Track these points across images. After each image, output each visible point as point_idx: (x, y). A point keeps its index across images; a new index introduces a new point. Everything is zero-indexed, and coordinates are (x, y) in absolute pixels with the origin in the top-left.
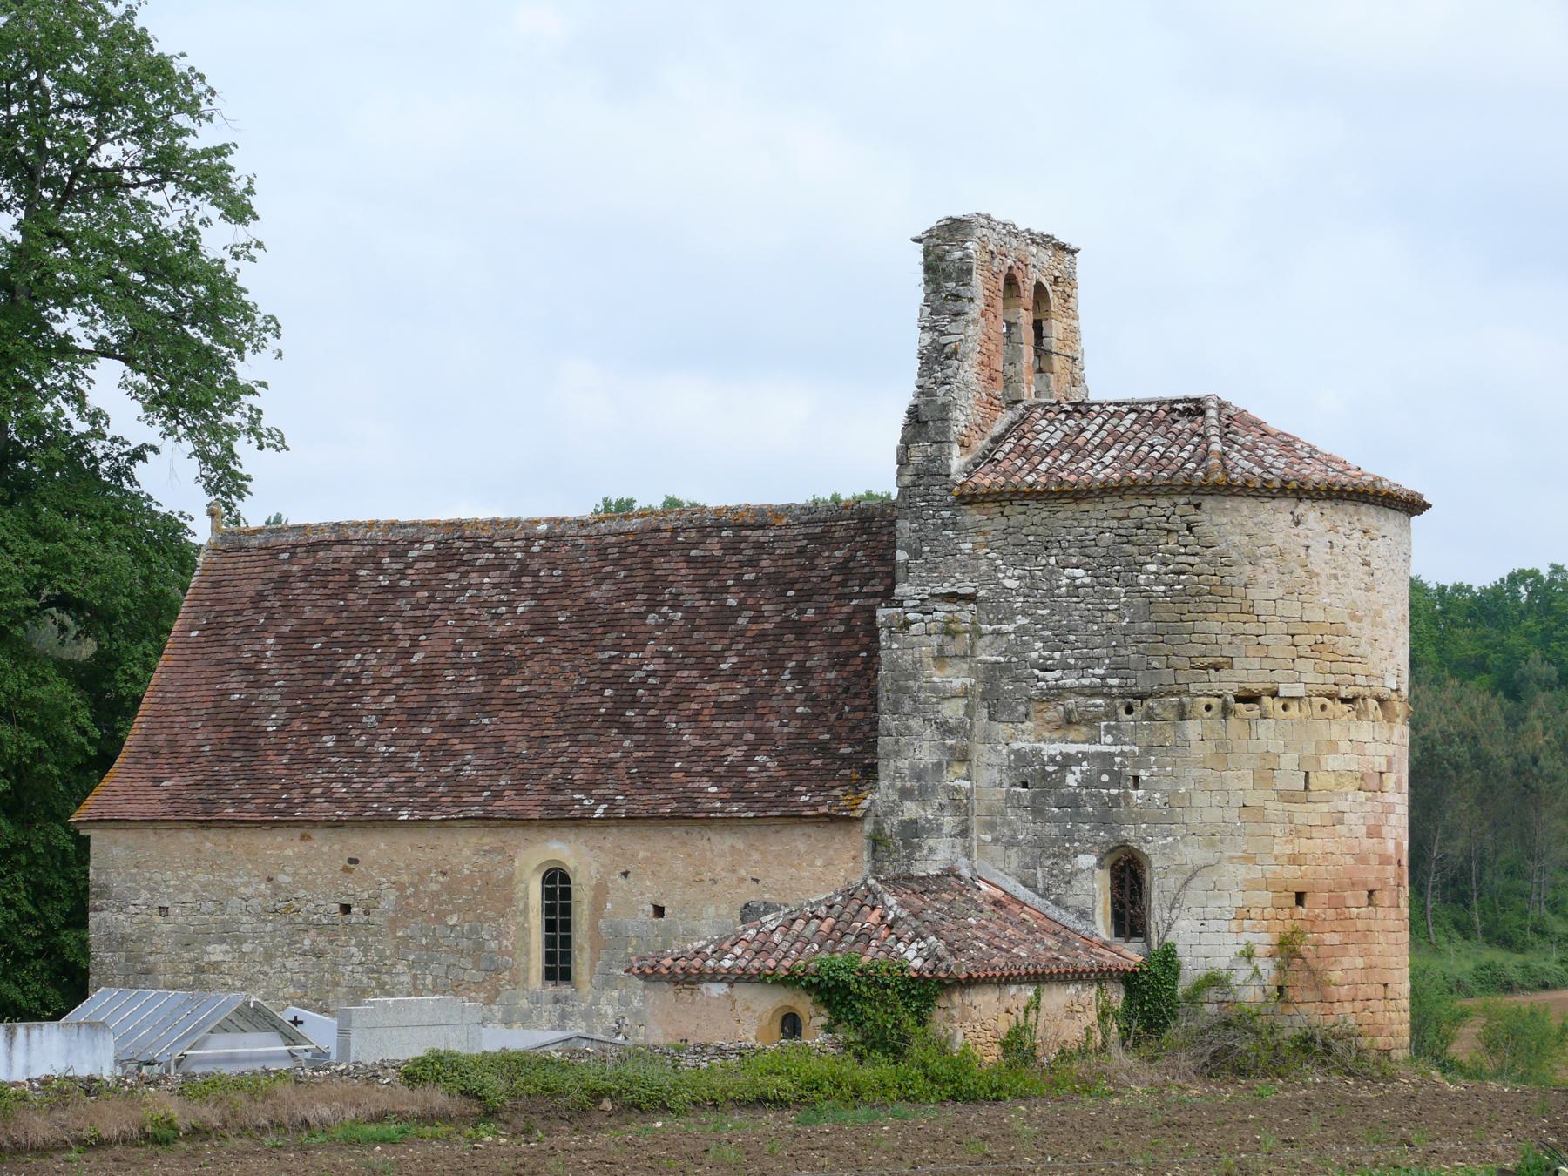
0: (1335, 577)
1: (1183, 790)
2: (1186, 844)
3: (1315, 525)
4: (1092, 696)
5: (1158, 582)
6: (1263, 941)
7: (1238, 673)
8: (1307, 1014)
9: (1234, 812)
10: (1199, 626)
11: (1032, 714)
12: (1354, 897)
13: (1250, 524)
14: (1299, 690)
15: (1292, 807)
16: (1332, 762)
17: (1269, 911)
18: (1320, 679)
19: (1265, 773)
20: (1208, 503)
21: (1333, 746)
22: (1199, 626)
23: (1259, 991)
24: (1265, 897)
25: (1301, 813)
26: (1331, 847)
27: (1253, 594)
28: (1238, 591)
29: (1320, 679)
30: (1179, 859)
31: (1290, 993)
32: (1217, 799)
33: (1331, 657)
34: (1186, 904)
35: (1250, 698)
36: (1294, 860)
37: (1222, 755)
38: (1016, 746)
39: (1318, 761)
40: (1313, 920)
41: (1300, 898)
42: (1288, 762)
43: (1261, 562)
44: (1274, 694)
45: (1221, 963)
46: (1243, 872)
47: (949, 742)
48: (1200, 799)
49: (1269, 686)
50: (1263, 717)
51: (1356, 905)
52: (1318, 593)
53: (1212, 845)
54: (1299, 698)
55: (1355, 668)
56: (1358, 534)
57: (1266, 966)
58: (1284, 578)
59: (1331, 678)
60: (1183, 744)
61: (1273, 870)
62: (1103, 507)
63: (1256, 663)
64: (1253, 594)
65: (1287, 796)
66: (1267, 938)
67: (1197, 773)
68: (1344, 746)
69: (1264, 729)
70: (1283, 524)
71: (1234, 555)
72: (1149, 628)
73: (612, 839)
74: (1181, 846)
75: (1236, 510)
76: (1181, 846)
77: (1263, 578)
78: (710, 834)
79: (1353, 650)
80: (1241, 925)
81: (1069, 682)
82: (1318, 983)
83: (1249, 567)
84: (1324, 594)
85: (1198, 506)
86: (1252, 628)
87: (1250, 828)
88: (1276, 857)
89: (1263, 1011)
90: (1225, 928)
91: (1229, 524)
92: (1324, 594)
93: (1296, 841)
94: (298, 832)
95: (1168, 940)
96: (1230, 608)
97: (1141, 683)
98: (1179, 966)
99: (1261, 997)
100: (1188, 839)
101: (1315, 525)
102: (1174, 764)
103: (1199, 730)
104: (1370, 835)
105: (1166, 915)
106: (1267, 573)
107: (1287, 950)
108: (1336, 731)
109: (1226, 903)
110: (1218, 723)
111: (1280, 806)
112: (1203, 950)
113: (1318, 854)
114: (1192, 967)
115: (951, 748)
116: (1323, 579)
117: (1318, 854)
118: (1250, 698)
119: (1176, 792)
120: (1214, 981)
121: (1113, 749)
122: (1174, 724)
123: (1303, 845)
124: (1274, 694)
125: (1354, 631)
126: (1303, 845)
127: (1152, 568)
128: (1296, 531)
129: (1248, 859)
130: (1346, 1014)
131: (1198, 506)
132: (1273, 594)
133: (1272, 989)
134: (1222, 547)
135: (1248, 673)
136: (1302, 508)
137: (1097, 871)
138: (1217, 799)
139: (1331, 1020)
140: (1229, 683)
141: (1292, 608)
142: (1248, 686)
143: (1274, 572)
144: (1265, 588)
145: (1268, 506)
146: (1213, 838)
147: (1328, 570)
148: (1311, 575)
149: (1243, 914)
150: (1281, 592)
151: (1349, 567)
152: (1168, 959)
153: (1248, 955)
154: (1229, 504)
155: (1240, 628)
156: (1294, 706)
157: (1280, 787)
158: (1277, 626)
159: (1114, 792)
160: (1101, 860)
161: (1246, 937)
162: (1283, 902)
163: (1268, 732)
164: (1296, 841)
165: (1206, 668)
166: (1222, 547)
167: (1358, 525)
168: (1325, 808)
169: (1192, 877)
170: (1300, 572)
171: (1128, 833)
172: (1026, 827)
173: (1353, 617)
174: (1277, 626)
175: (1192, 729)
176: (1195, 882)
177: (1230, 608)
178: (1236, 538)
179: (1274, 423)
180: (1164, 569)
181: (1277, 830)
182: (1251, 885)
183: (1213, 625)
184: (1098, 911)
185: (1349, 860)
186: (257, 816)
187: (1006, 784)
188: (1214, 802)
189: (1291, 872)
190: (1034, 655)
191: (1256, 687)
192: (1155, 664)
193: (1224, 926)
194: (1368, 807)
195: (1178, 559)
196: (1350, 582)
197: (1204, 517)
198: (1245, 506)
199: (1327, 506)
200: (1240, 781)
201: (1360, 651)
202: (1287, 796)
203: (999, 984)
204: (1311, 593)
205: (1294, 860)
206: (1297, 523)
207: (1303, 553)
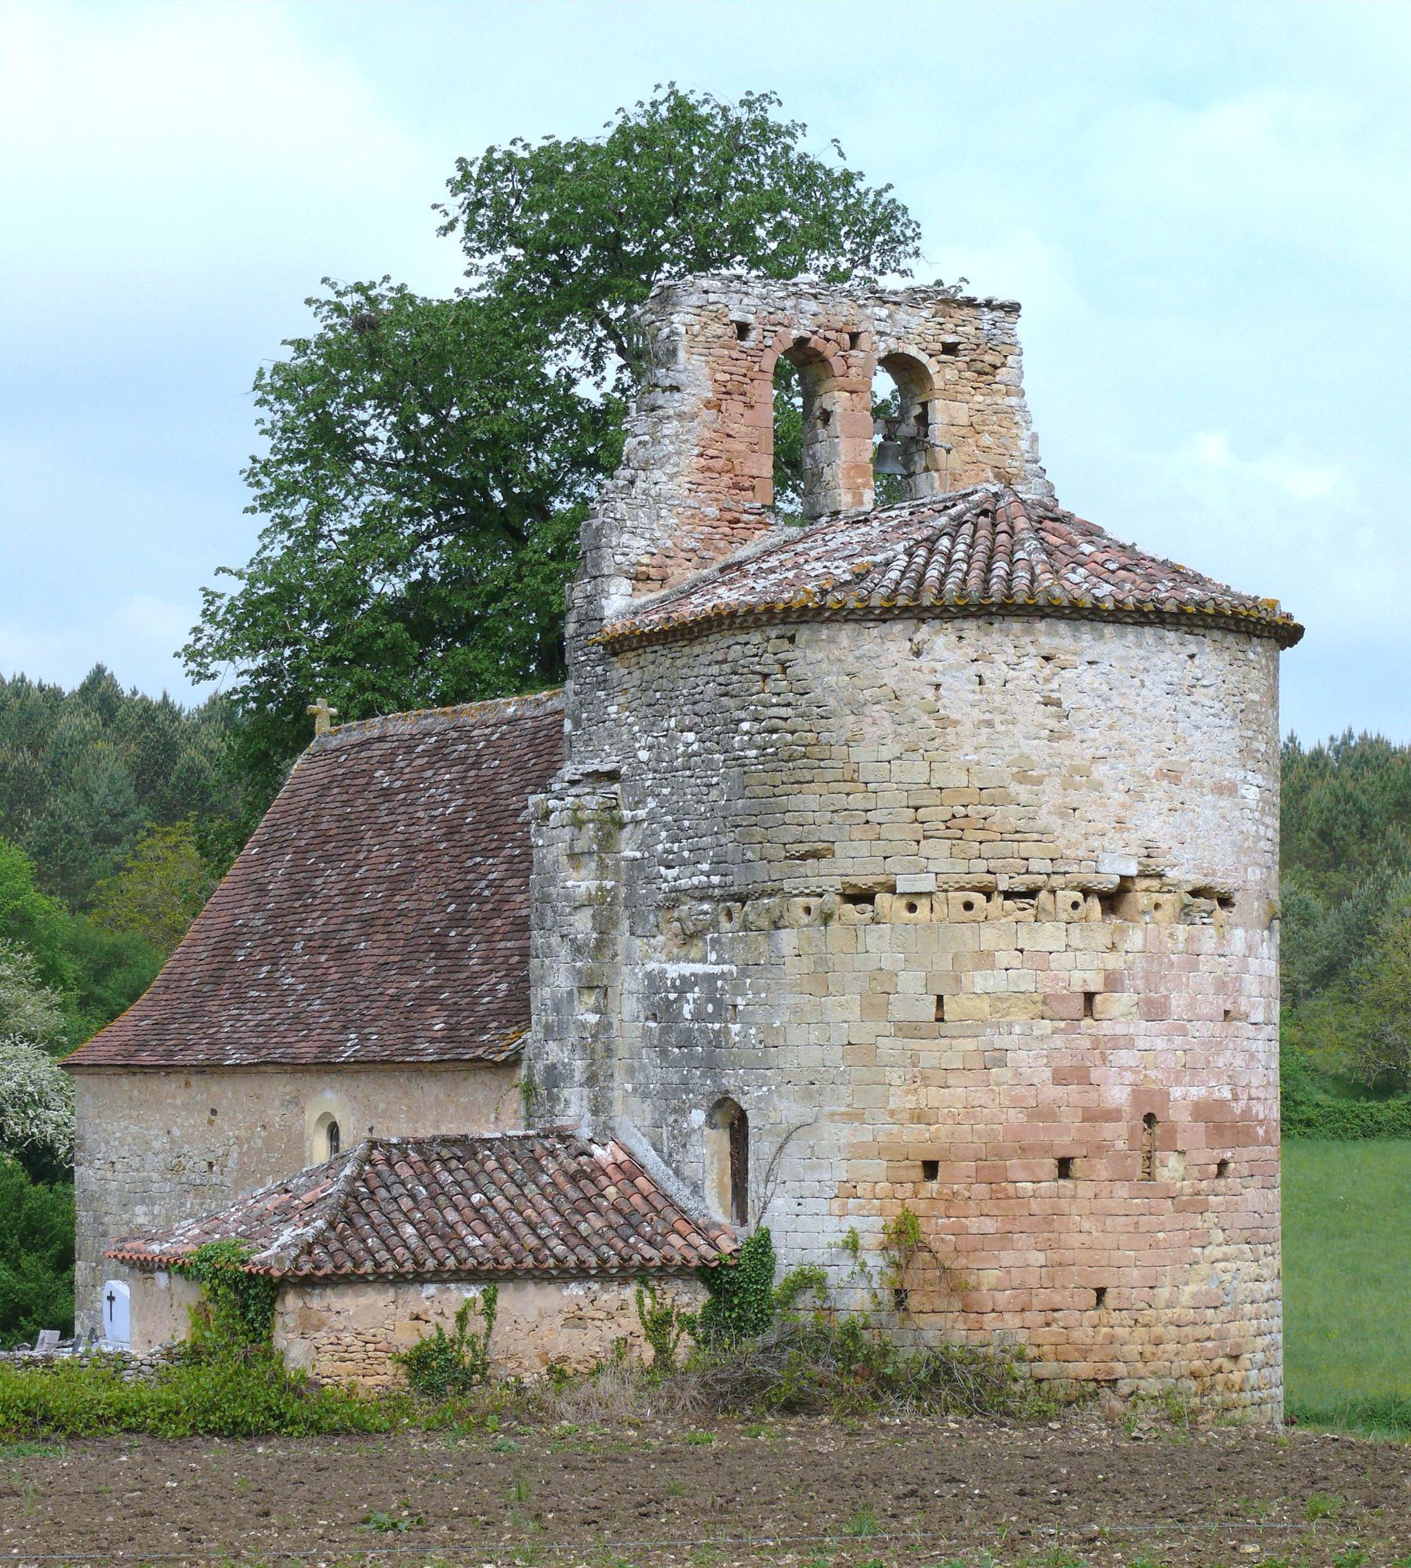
0: (990, 724)
1: (777, 1024)
2: (780, 1097)
3: (946, 654)
4: (701, 899)
5: (751, 745)
6: (871, 1228)
7: (840, 862)
8: (939, 1329)
9: (837, 1052)
10: (794, 802)
11: (663, 926)
12: (1026, 1167)
13: (851, 659)
14: (927, 883)
15: (916, 1044)
16: (980, 981)
17: (883, 1187)
18: (962, 866)
19: (878, 996)
20: (804, 634)
21: (985, 959)
22: (794, 802)
23: (867, 1295)
24: (878, 1167)
25: (931, 1053)
26: (980, 1097)
27: (858, 754)
28: (839, 751)
29: (962, 866)
30: (774, 1117)
31: (913, 1302)
32: (815, 1035)
33: (981, 835)
34: (782, 1177)
35: (861, 897)
36: (919, 1116)
37: (822, 976)
38: (649, 967)
39: (958, 980)
40: (951, 1199)
41: (931, 1169)
42: (910, 982)
43: (866, 710)
44: (892, 889)
45: (818, 1256)
46: (845, 1133)
47: (579, 964)
48: (796, 1035)
49: (882, 879)
50: (875, 921)
51: (1035, 1185)
52: (957, 747)
53: (809, 1096)
54: (930, 894)
55: (1025, 849)
56: (1032, 663)
57: (874, 1261)
58: (901, 730)
59: (983, 865)
60: (777, 962)
61: (887, 1130)
62: (709, 648)
63: (864, 848)
64: (858, 754)
65: (909, 1030)
66: (878, 1223)
67: (792, 999)
68: (1003, 958)
69: (876, 939)
70: (896, 657)
71: (832, 702)
72: (744, 807)
73: (365, 1086)
74: (775, 1099)
75: (832, 640)
76: (775, 1099)
77: (872, 732)
78: (423, 1083)
79: (1022, 825)
80: (844, 1206)
81: (684, 883)
82: (957, 1289)
83: (852, 718)
84: (968, 748)
85: (792, 640)
86: (857, 801)
87: (859, 1073)
88: (892, 1113)
89: (872, 1321)
90: (824, 1211)
91: (829, 659)
92: (968, 748)
93: (922, 1091)
94: (182, 1078)
95: (763, 1224)
96: (829, 775)
97: (738, 881)
98: (773, 1260)
99: (869, 1306)
100: (784, 1088)
101: (946, 654)
102: (768, 990)
103: (795, 942)
104: (1060, 1078)
105: (762, 1190)
106: (878, 723)
107: (904, 1238)
108: (988, 937)
109: (826, 1176)
110: (816, 932)
111: (899, 1043)
112: (800, 1238)
113: (958, 1108)
114: (787, 1259)
115: (579, 972)
116: (966, 729)
117: (958, 1108)
118: (861, 897)
119: (770, 1026)
120: (809, 1281)
121: (717, 969)
122: (769, 936)
123: (932, 1096)
124: (892, 889)
125: (1023, 798)
126: (932, 1096)
127: (745, 726)
128: (917, 663)
129: (854, 1116)
130: (1004, 1328)
131: (792, 640)
132: (885, 753)
133: (886, 1296)
134: (817, 693)
135: (855, 863)
136: (924, 632)
137: (707, 1130)
138: (815, 1035)
139: (976, 1338)
140: (829, 876)
141: (916, 771)
142: (853, 880)
143: (887, 723)
144: (873, 743)
145: (875, 632)
146: (810, 1088)
147: (976, 714)
148: (945, 723)
149: (848, 1191)
150: (897, 749)
151: (1016, 708)
152: (762, 1246)
153: (852, 1245)
154: (825, 633)
155: (841, 801)
156: (923, 905)
157: (898, 1017)
158: (893, 796)
159: (717, 1026)
160: (709, 1116)
161: (852, 1222)
162: (902, 1175)
163: (882, 942)
164: (922, 1091)
165: (803, 857)
166: (817, 693)
167: (1031, 649)
168: (970, 1044)
169: (787, 1140)
170: (925, 719)
171: (729, 1081)
172: (657, 1075)
173: (1023, 777)
174: (893, 796)
175: (787, 939)
176: (790, 1148)
177: (829, 775)
178: (831, 680)
179: (1118, 531)
180: (757, 726)
181: (894, 1075)
182: (858, 1152)
183: (808, 800)
184: (708, 1183)
185: (1016, 1117)
186: (435, 1057)
187: (642, 1019)
188: (812, 1039)
189: (913, 1134)
190: (660, 847)
191: (864, 882)
192: (749, 855)
193: (822, 1206)
194: (1058, 1041)
195: (775, 711)
196: (1014, 729)
197: (798, 653)
198: (845, 634)
199: (970, 628)
200: (844, 1008)
201: (1039, 824)
202: (909, 1030)
203: (393, 1283)
204: (946, 748)
205: (919, 1116)
206: (918, 654)
207: (930, 694)
